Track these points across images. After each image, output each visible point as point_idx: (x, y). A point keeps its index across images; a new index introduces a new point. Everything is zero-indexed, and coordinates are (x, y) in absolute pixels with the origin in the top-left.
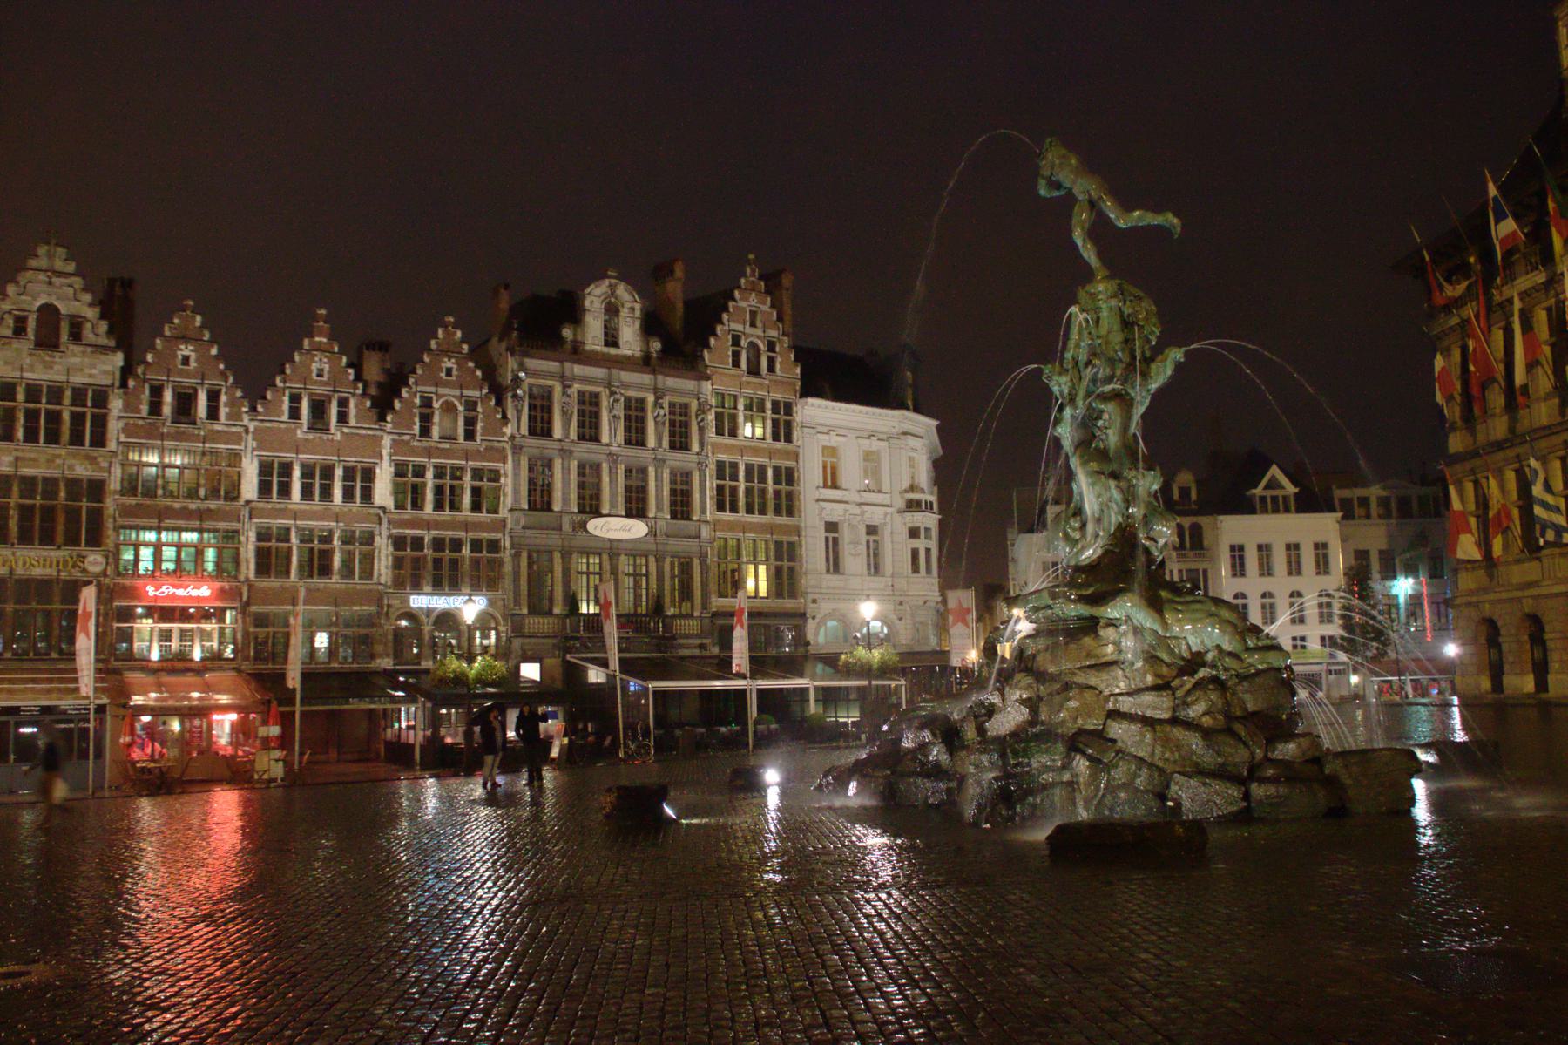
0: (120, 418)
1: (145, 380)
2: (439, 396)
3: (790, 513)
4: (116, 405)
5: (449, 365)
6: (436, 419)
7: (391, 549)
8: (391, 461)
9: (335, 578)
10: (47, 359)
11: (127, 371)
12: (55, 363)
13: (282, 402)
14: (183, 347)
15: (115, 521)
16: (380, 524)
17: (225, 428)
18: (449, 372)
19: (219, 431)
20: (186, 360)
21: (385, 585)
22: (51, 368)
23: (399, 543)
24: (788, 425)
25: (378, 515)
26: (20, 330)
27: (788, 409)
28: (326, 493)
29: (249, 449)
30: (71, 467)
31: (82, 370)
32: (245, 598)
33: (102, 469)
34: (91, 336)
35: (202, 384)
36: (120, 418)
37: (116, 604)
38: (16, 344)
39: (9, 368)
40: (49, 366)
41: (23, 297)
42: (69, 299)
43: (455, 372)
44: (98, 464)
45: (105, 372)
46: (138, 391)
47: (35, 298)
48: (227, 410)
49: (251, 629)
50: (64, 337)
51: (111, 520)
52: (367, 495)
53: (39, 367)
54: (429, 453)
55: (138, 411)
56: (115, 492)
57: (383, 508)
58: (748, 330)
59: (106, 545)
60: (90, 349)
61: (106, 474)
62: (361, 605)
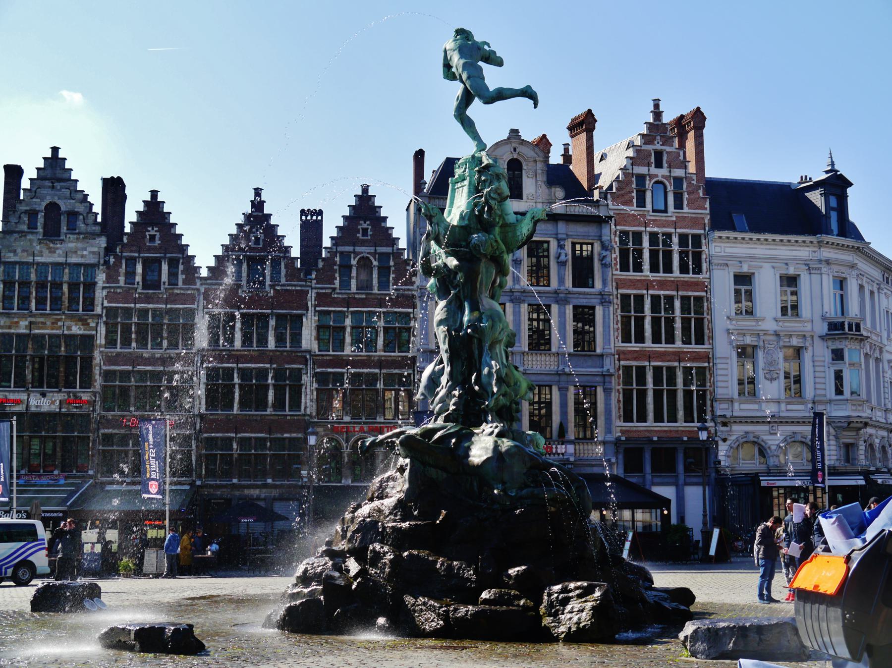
0: (104, 288)
1: (121, 257)
2: (356, 254)
3: (700, 341)
4: (101, 277)
5: (365, 226)
6: (354, 273)
7: (315, 385)
8: (316, 311)
9: (269, 411)
10: (51, 245)
11: (109, 250)
12: (57, 248)
14: (150, 229)
15: (100, 367)
16: (307, 365)
17: (182, 292)
18: (365, 231)
20: (152, 238)
21: (310, 416)
22: (55, 252)
23: (321, 378)
24: (697, 257)
25: (305, 357)
26: (32, 226)
27: (697, 239)
28: (263, 341)
29: (201, 307)
30: (69, 328)
31: (76, 252)
32: (198, 427)
33: (91, 329)
35: (165, 258)
36: (104, 288)
37: (102, 431)
38: (30, 237)
39: (25, 254)
40: (52, 251)
41: (34, 200)
42: (66, 198)
43: (370, 233)
44: (88, 324)
45: (93, 253)
46: (118, 264)
47: (42, 200)
48: (184, 276)
49: (204, 452)
50: (64, 229)
51: (97, 368)
52: (297, 338)
53: (46, 252)
54: (349, 302)
55: (118, 282)
56: (101, 346)
57: (309, 352)
58: (654, 170)
59: (95, 387)
60: (82, 236)
61: (94, 332)
62: (290, 432)
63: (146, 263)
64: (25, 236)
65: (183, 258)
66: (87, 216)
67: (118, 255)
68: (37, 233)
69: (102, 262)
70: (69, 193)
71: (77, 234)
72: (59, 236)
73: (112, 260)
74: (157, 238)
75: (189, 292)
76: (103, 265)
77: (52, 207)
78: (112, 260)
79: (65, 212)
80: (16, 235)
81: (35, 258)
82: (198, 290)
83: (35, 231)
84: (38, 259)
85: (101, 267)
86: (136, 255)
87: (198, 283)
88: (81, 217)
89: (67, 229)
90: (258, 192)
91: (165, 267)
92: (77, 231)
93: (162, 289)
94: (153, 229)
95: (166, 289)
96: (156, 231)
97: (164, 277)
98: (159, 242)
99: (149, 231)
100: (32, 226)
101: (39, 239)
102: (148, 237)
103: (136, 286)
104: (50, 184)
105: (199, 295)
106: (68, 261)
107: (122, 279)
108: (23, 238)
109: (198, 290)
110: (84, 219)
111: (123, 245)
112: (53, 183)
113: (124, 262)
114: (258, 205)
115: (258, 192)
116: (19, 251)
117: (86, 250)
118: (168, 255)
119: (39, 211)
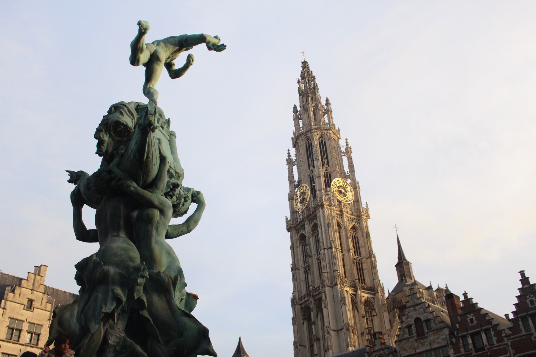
1: (459, 337)
10: (422, 341)
12: (425, 342)
13: (519, 325)
14: (469, 316)
17: (498, 348)
19: (495, 350)
20: (472, 320)
22: (424, 344)
26: (410, 333)
31: (434, 341)
34: (434, 325)
35: (482, 330)
38: (411, 340)
40: (423, 344)
41: (408, 319)
42: (422, 313)
45: (443, 339)
46: (458, 342)
47: (412, 318)
48: (496, 338)
50: (426, 330)
53: (420, 345)
55: (460, 352)
63: (472, 335)
64: (409, 340)
65: (492, 327)
66: (435, 320)
67: (456, 336)
68: (413, 337)
69: (449, 342)
70: (423, 310)
71: (433, 331)
72: (424, 335)
73: (454, 340)
74: (474, 320)
75: (502, 347)
76: (450, 345)
77: (417, 320)
78: (454, 340)
79: (424, 321)
80: (404, 341)
81: (416, 351)
82: (507, 344)
83: (412, 336)
84: (418, 351)
85: (450, 346)
86: (466, 333)
87: (505, 339)
88: (432, 321)
89: (428, 330)
90: (522, 273)
91: (484, 336)
92: (432, 329)
93: (486, 349)
94: (470, 315)
95: (488, 349)
96: (472, 316)
97: (485, 342)
98: (476, 322)
99: (469, 317)
100: (410, 333)
101: (415, 340)
102: (469, 321)
103: (471, 352)
104: (414, 309)
105: (508, 347)
106: (432, 348)
107: (462, 350)
108: (408, 341)
109: (507, 344)
110: (434, 321)
111: (457, 329)
112: (414, 308)
113: (460, 339)
114: (525, 280)
115: (522, 273)
116: (408, 349)
117: (439, 339)
118: (483, 328)
119: (412, 325)
